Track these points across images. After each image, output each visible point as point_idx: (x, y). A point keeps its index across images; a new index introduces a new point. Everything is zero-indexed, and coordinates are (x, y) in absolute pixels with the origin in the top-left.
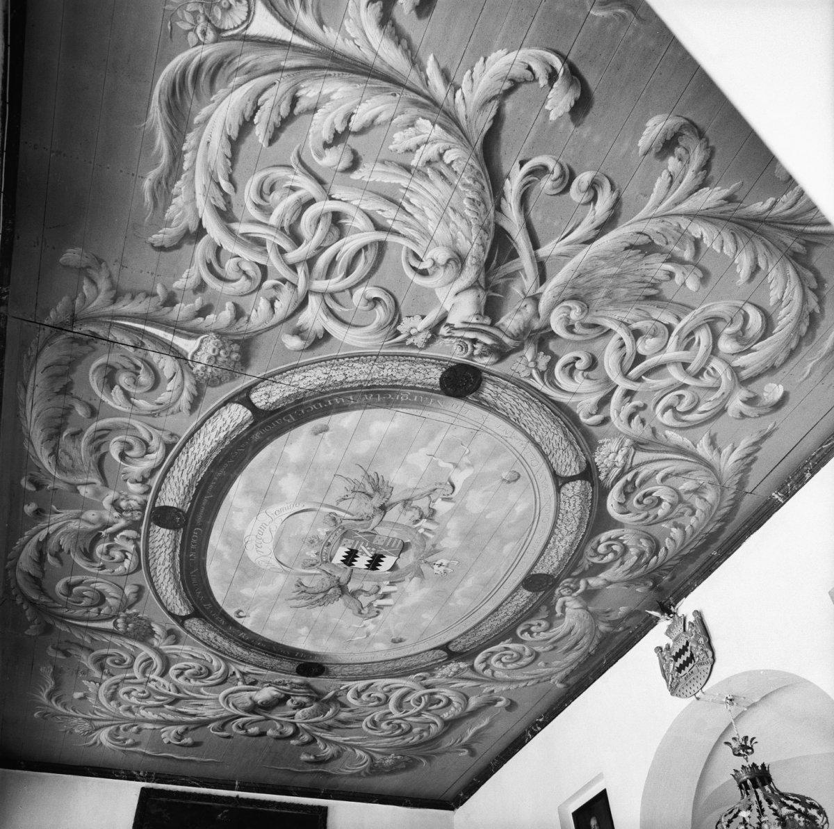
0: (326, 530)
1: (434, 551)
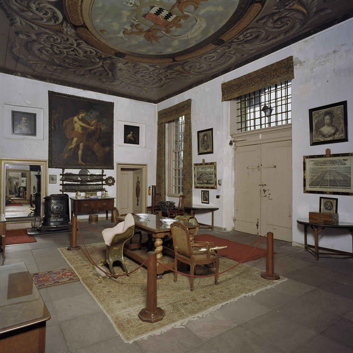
0: (172, 29)
1: (133, 11)
